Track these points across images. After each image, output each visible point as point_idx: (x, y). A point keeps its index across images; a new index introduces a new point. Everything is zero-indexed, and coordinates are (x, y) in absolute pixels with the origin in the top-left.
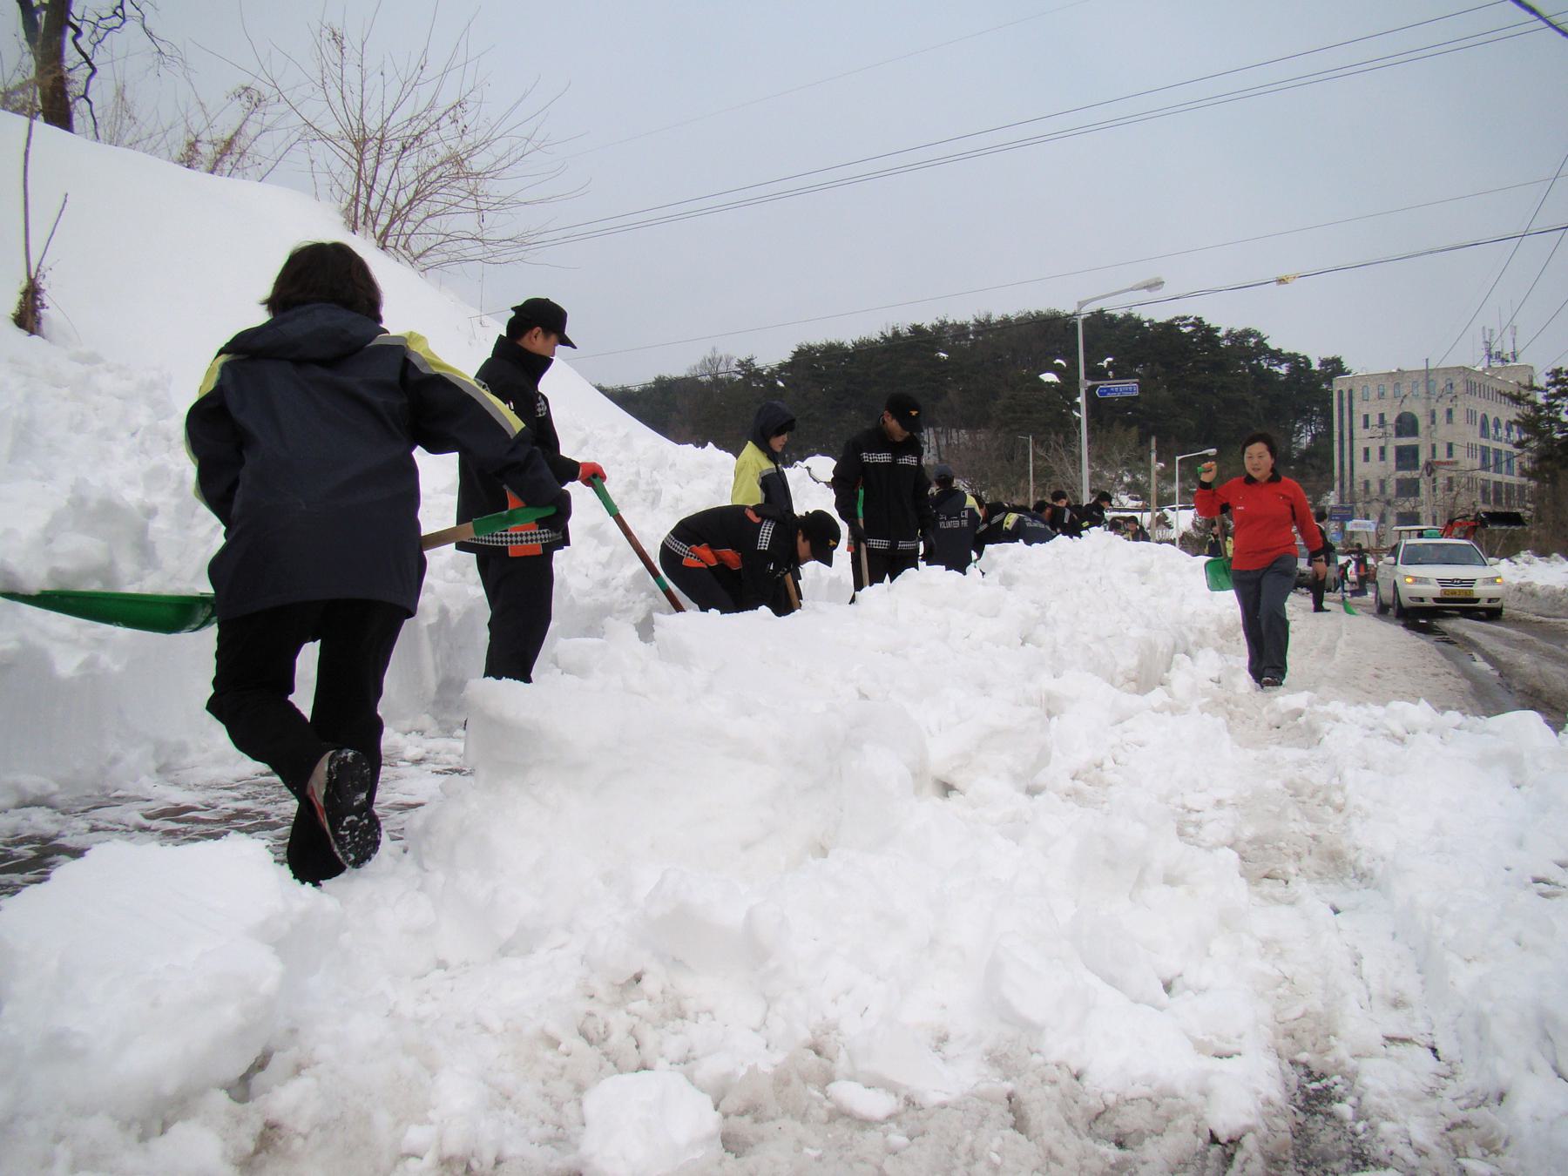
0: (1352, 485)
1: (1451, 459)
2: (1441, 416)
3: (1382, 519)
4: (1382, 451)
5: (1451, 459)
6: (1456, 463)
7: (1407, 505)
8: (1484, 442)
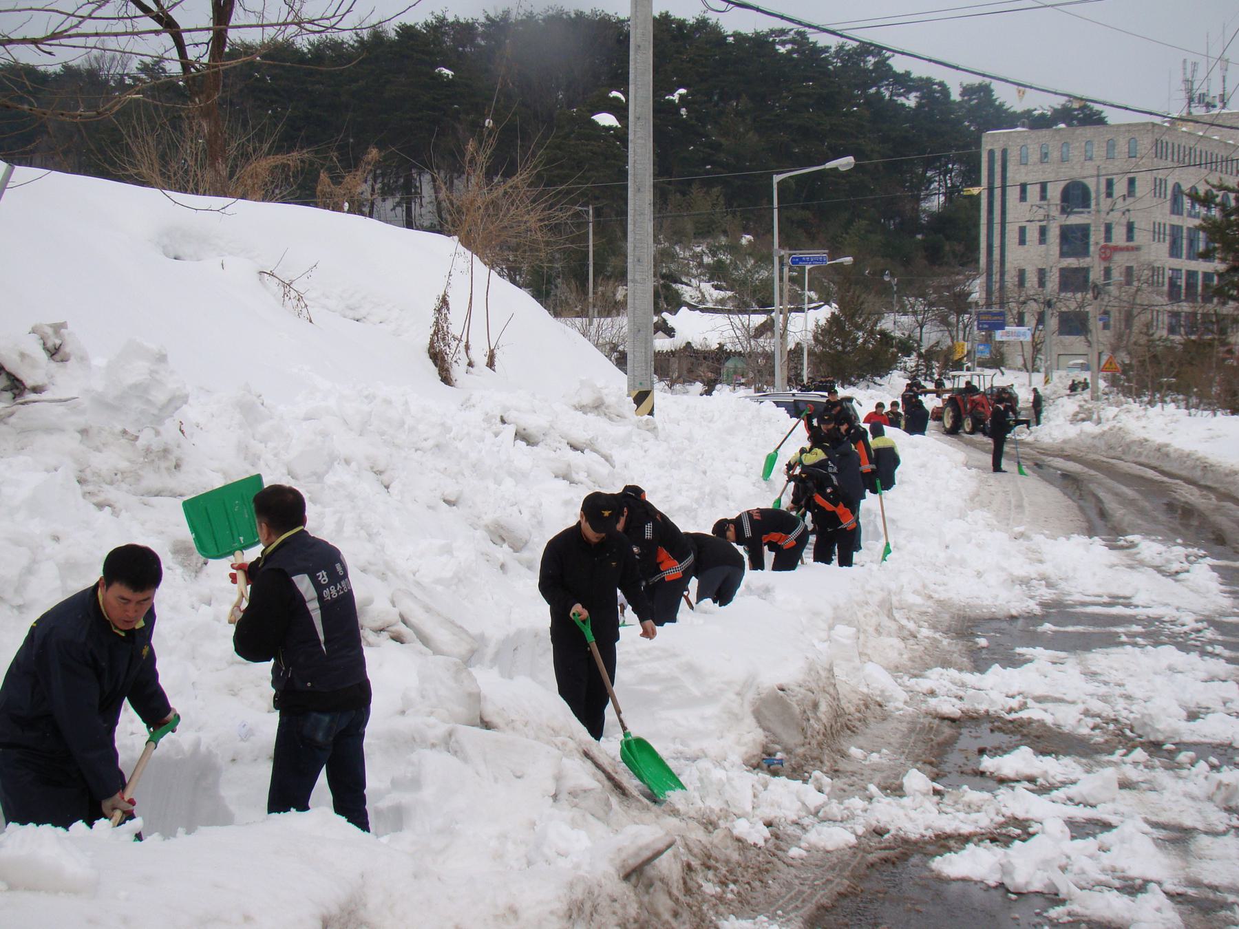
0: (1002, 274)
1: (1131, 244)
2: (1120, 188)
3: (1041, 320)
4: (1043, 232)
5: (1131, 244)
6: (1137, 249)
7: (1071, 301)
8: (1176, 220)
